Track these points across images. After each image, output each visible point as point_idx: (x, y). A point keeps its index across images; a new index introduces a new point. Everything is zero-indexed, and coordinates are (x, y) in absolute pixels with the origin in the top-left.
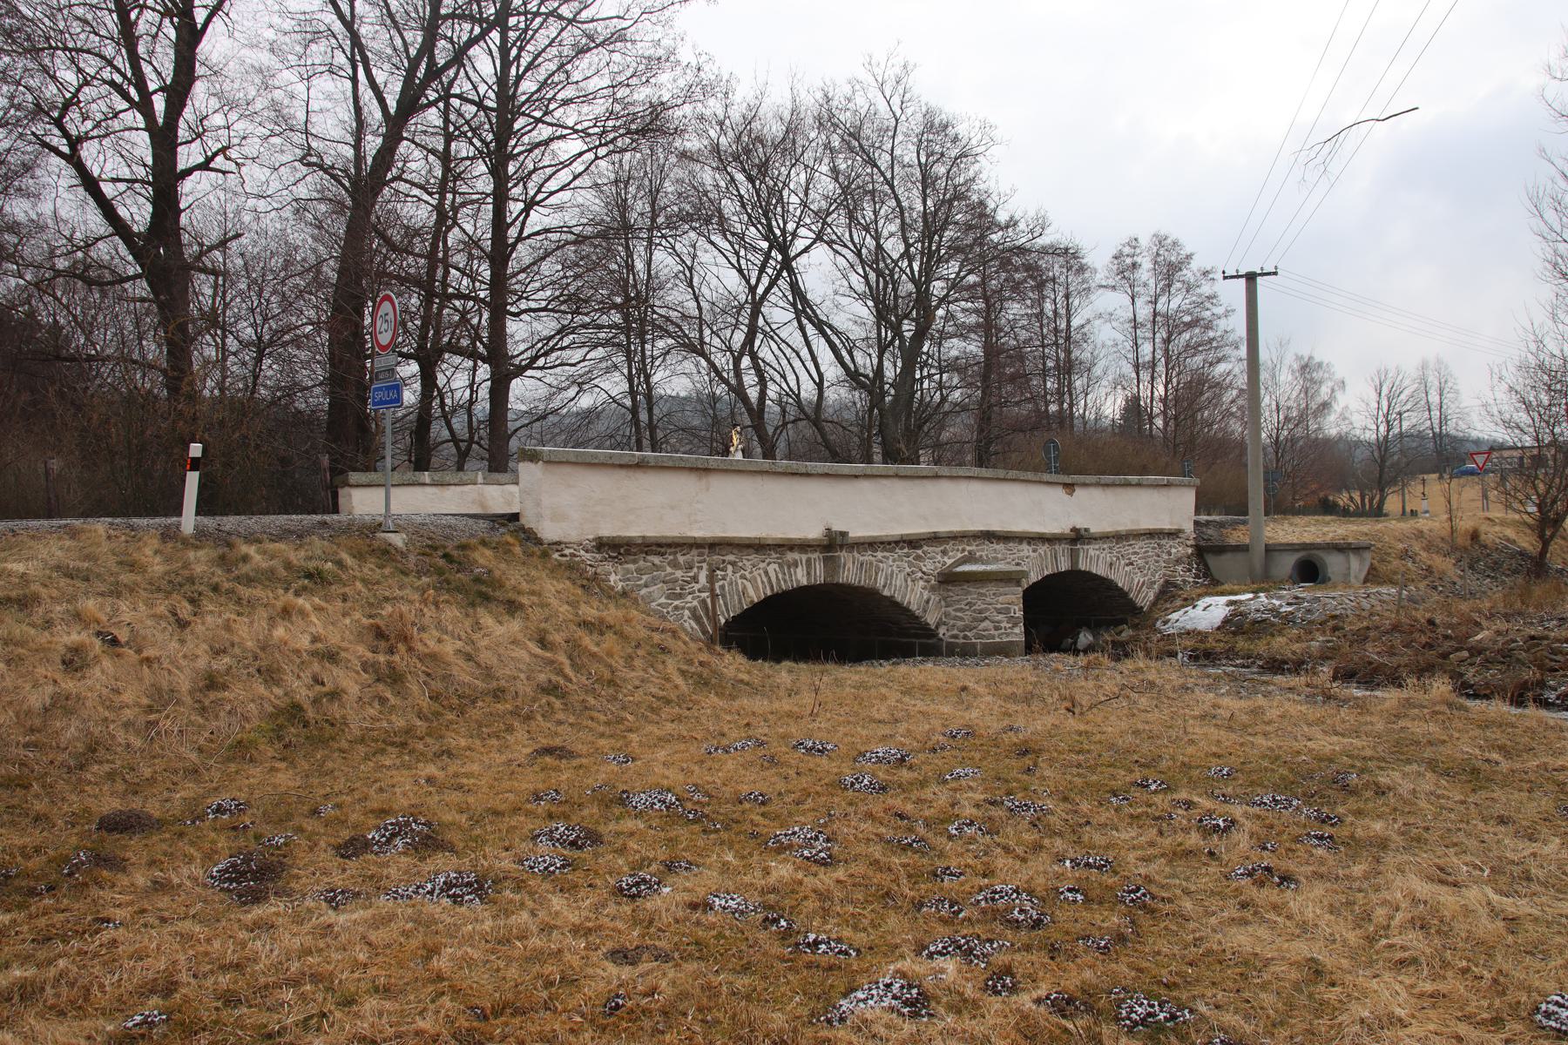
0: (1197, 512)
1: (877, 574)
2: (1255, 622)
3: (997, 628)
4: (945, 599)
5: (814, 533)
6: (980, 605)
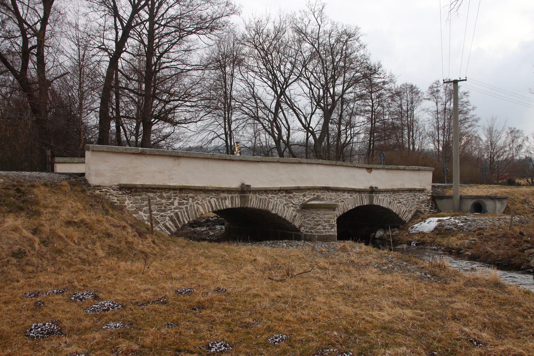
0: (433, 181)
1: (268, 204)
2: (447, 229)
3: (324, 229)
4: (304, 215)
5: (235, 184)
6: (317, 219)
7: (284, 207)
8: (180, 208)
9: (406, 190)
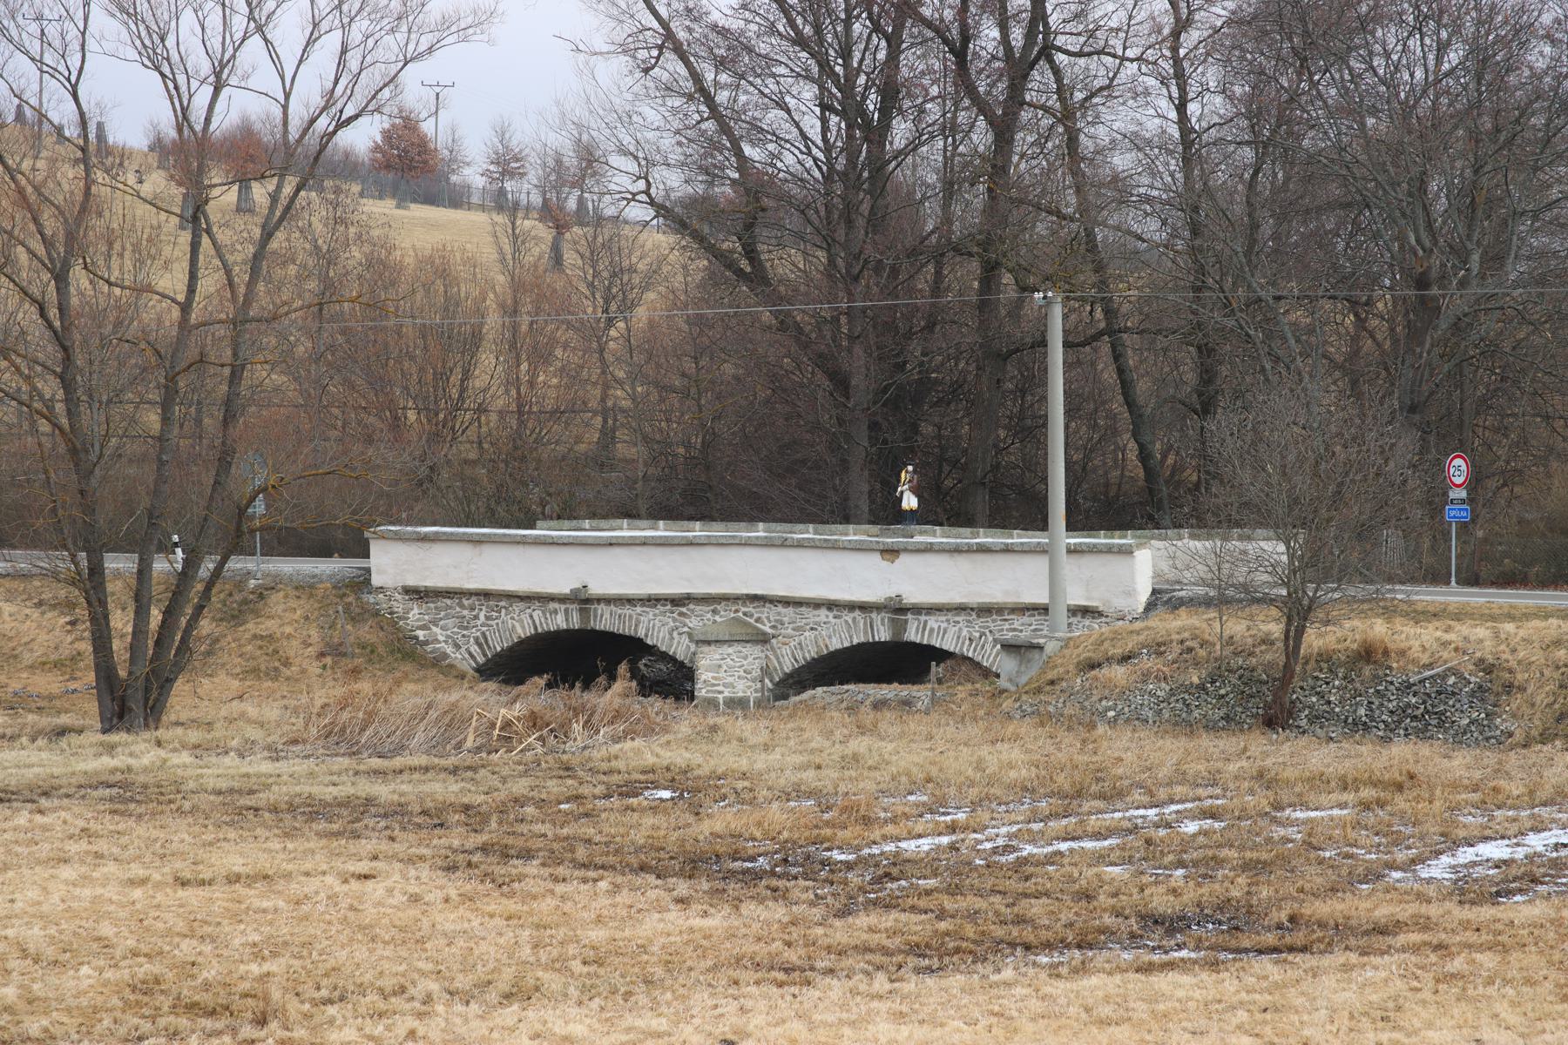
7: (671, 634)
8: (488, 626)
9: (1028, 609)
